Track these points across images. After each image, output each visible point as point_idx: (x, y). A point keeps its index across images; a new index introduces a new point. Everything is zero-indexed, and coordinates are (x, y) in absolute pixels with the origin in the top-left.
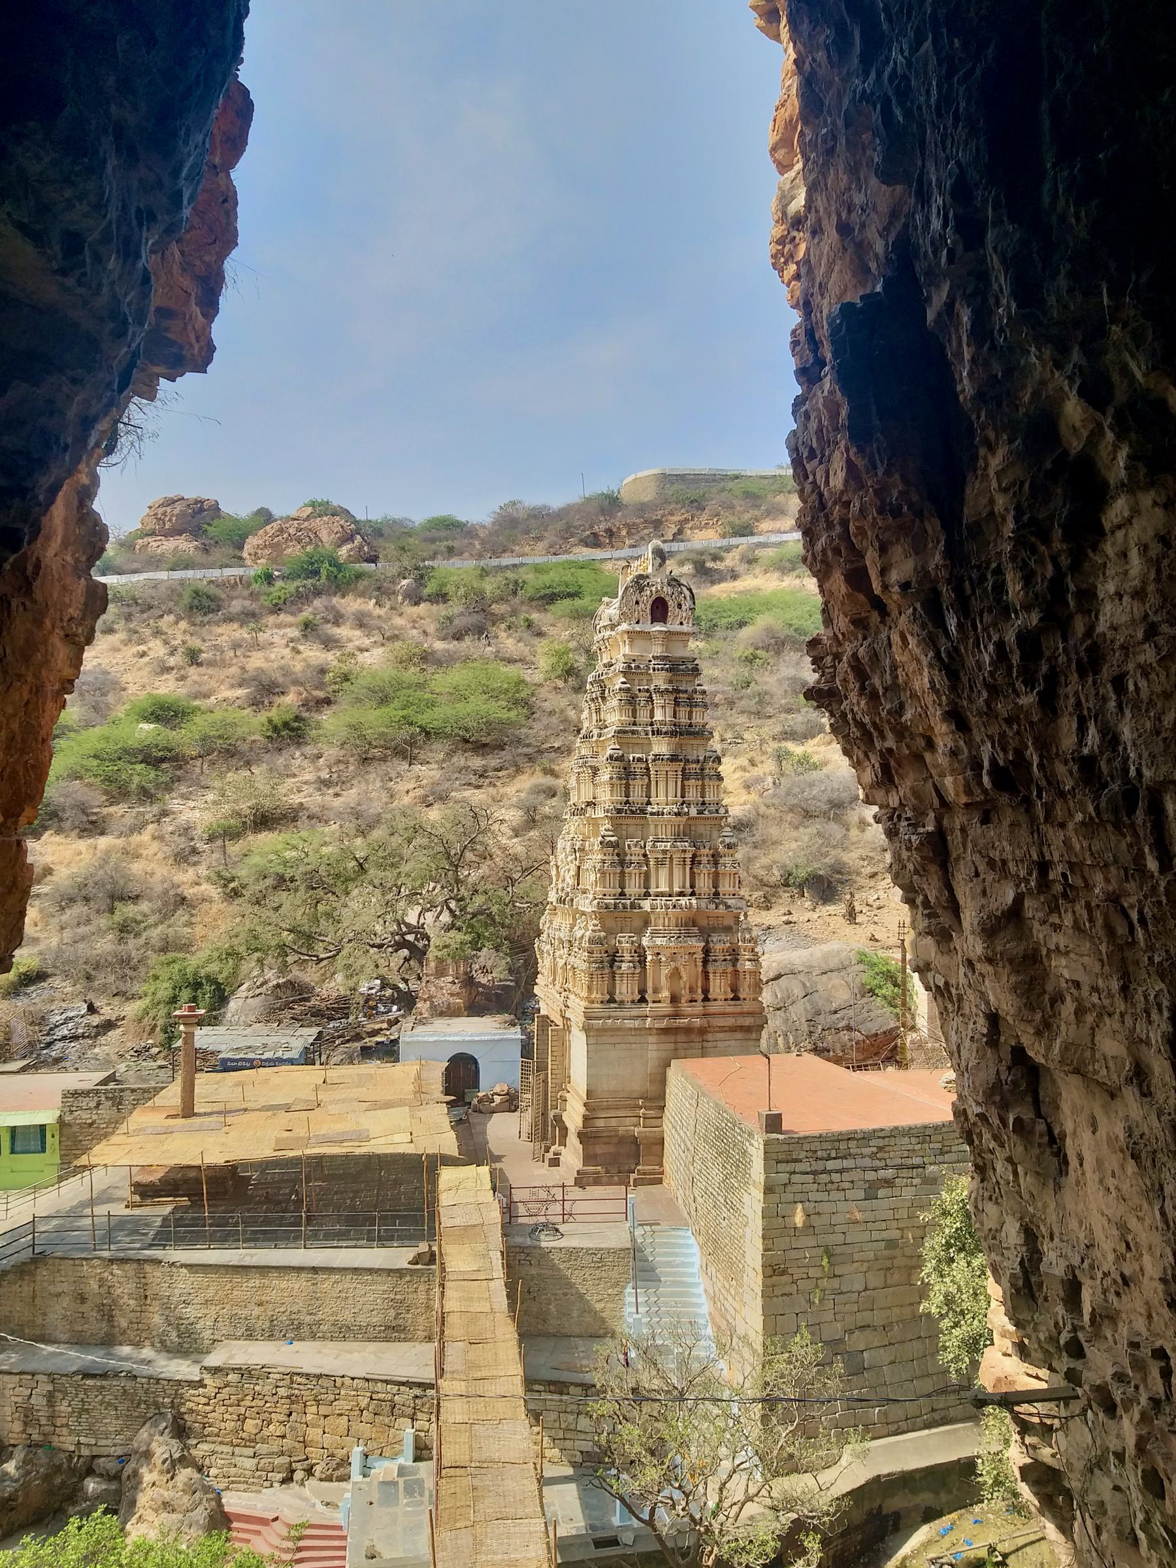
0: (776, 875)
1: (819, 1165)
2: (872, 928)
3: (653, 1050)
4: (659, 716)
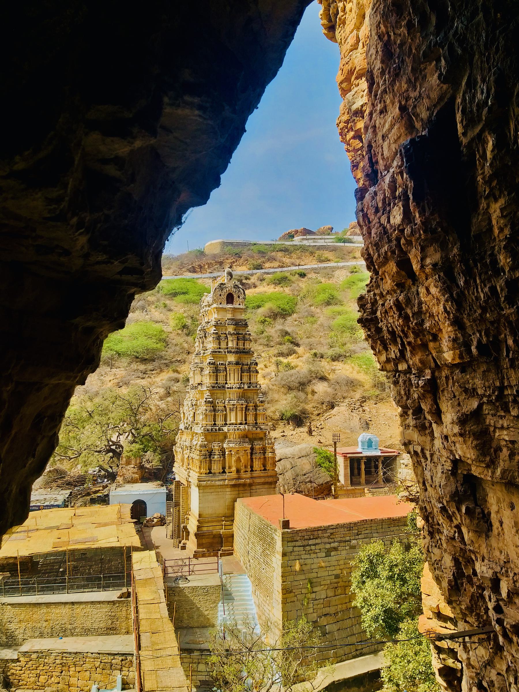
0: (277, 415)
1: (306, 543)
2: (319, 437)
3: (228, 494)
4: (230, 345)
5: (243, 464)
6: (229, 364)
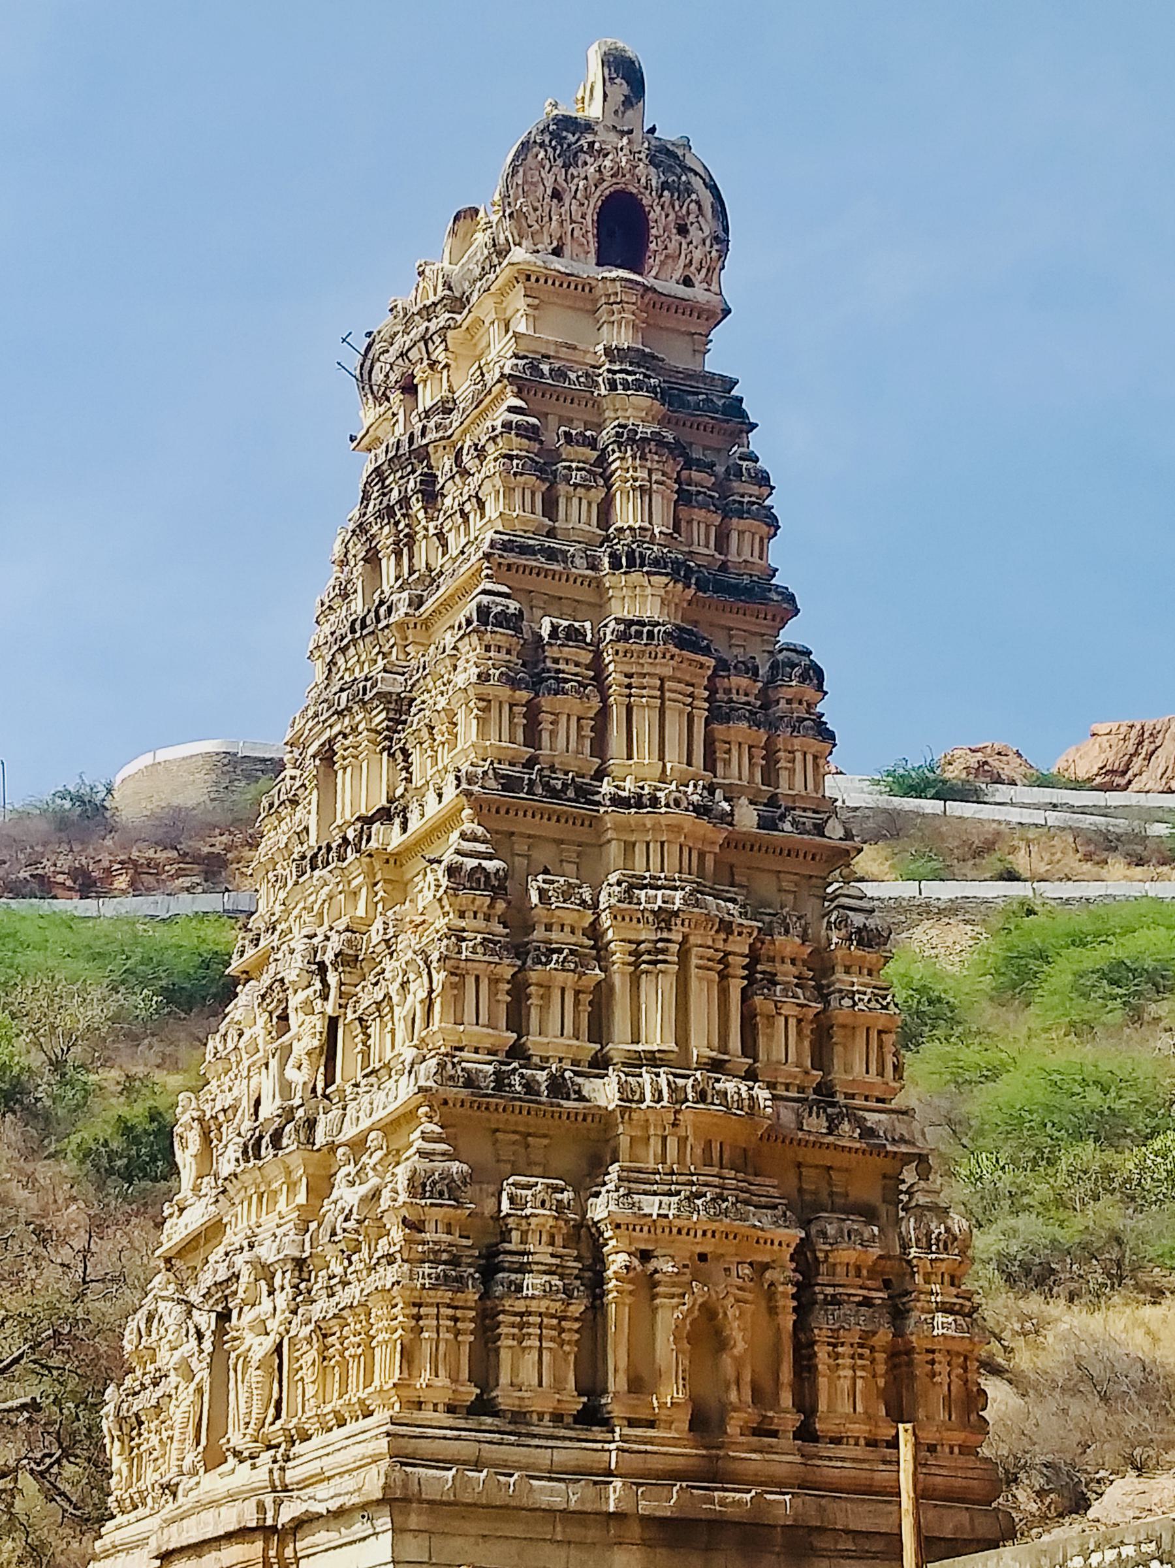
4: (626, 514)
5: (739, 1362)
6: (623, 637)
